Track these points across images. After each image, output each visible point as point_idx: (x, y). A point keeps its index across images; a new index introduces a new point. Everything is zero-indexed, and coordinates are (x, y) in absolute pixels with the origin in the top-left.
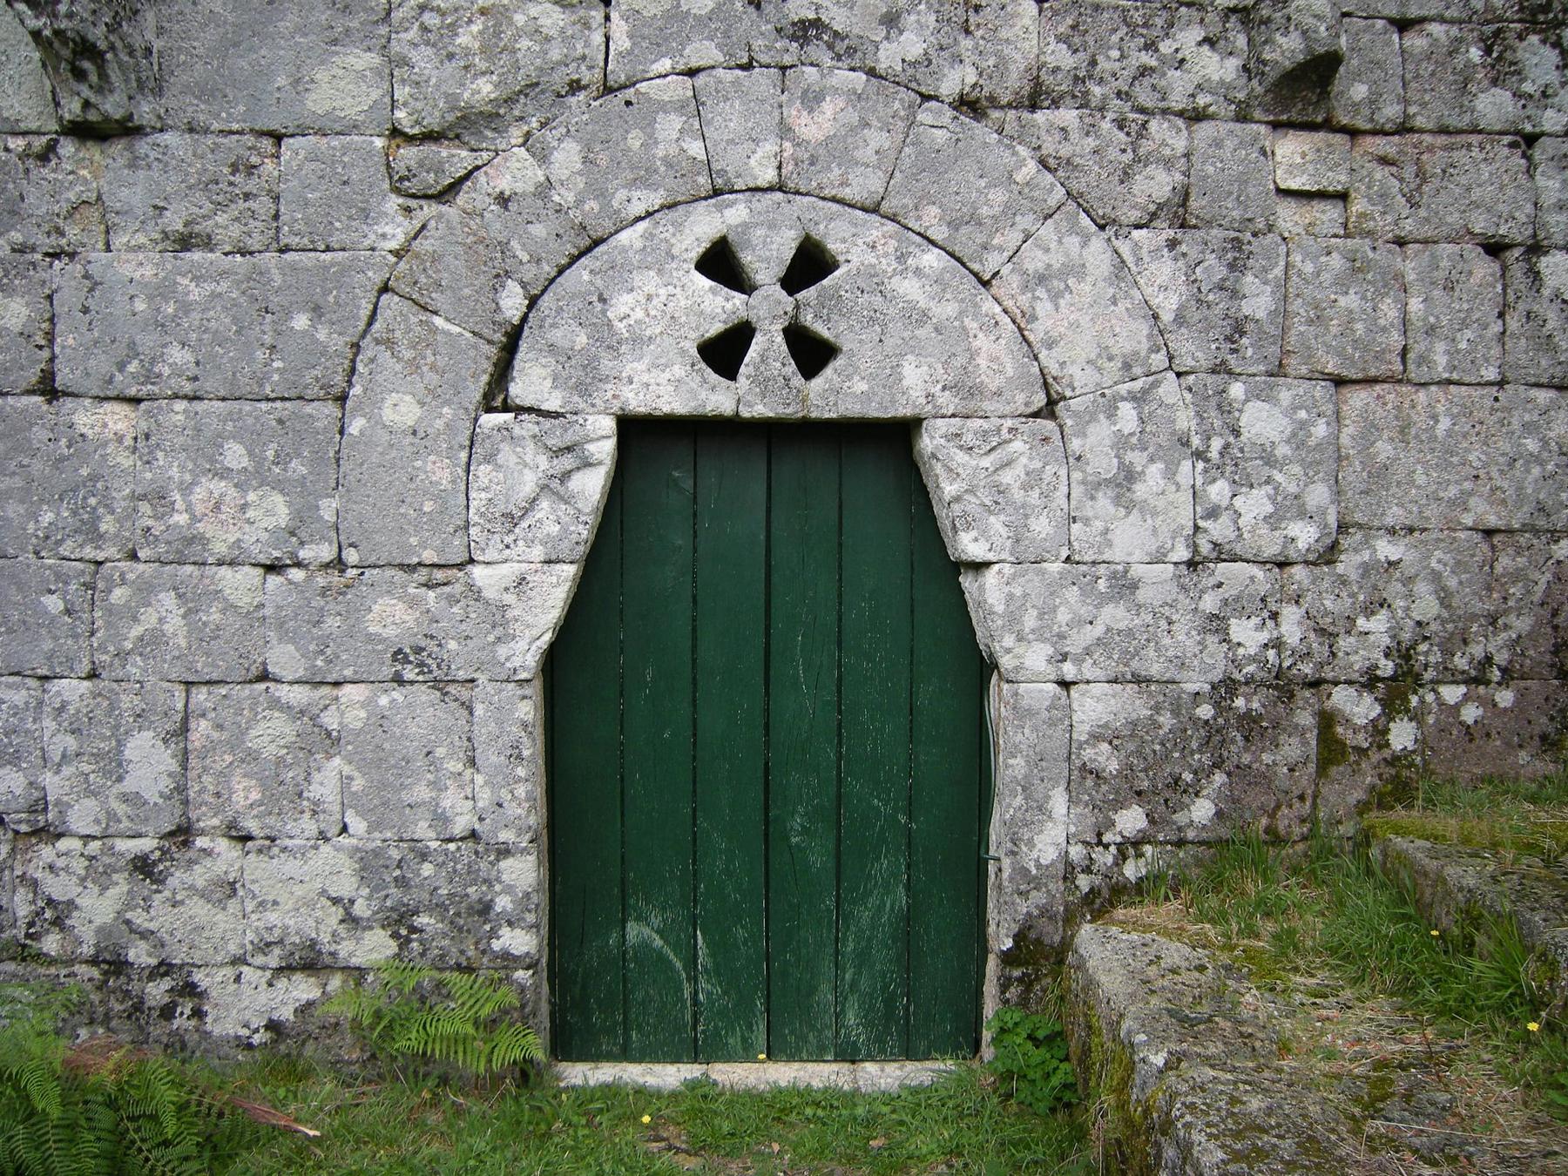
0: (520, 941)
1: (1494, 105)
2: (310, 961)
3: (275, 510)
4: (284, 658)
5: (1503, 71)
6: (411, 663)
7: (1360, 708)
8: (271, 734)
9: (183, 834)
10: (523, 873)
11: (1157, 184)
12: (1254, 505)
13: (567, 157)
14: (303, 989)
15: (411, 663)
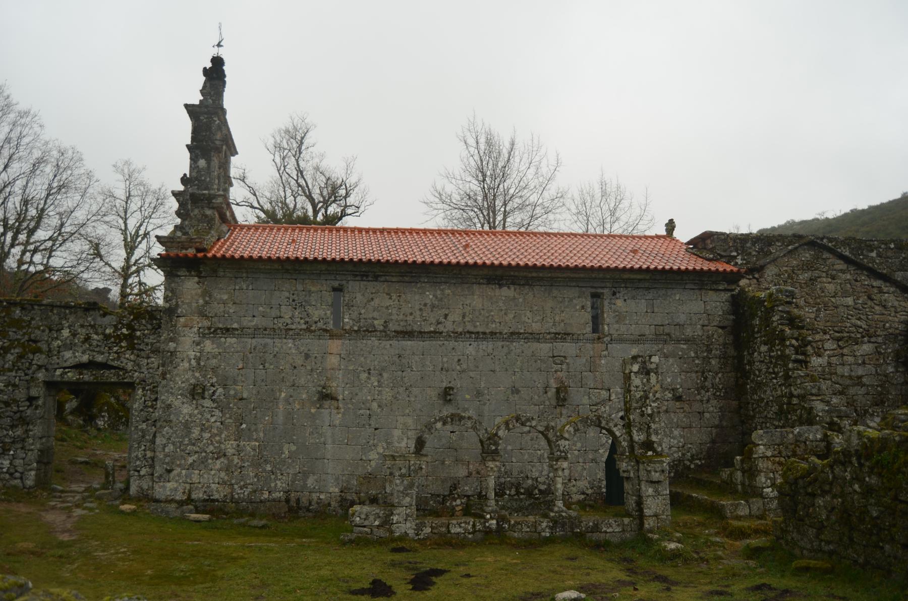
0: (604, 490)
1: (698, 397)
2: (583, 493)
3: (579, 445)
4: (581, 460)
5: (699, 394)
6: (593, 460)
7: (688, 463)
8: (579, 468)
9: (570, 480)
10: (604, 483)
11: (665, 408)
12: (676, 442)
13: (607, 408)
14: (583, 497)
15: (593, 460)
